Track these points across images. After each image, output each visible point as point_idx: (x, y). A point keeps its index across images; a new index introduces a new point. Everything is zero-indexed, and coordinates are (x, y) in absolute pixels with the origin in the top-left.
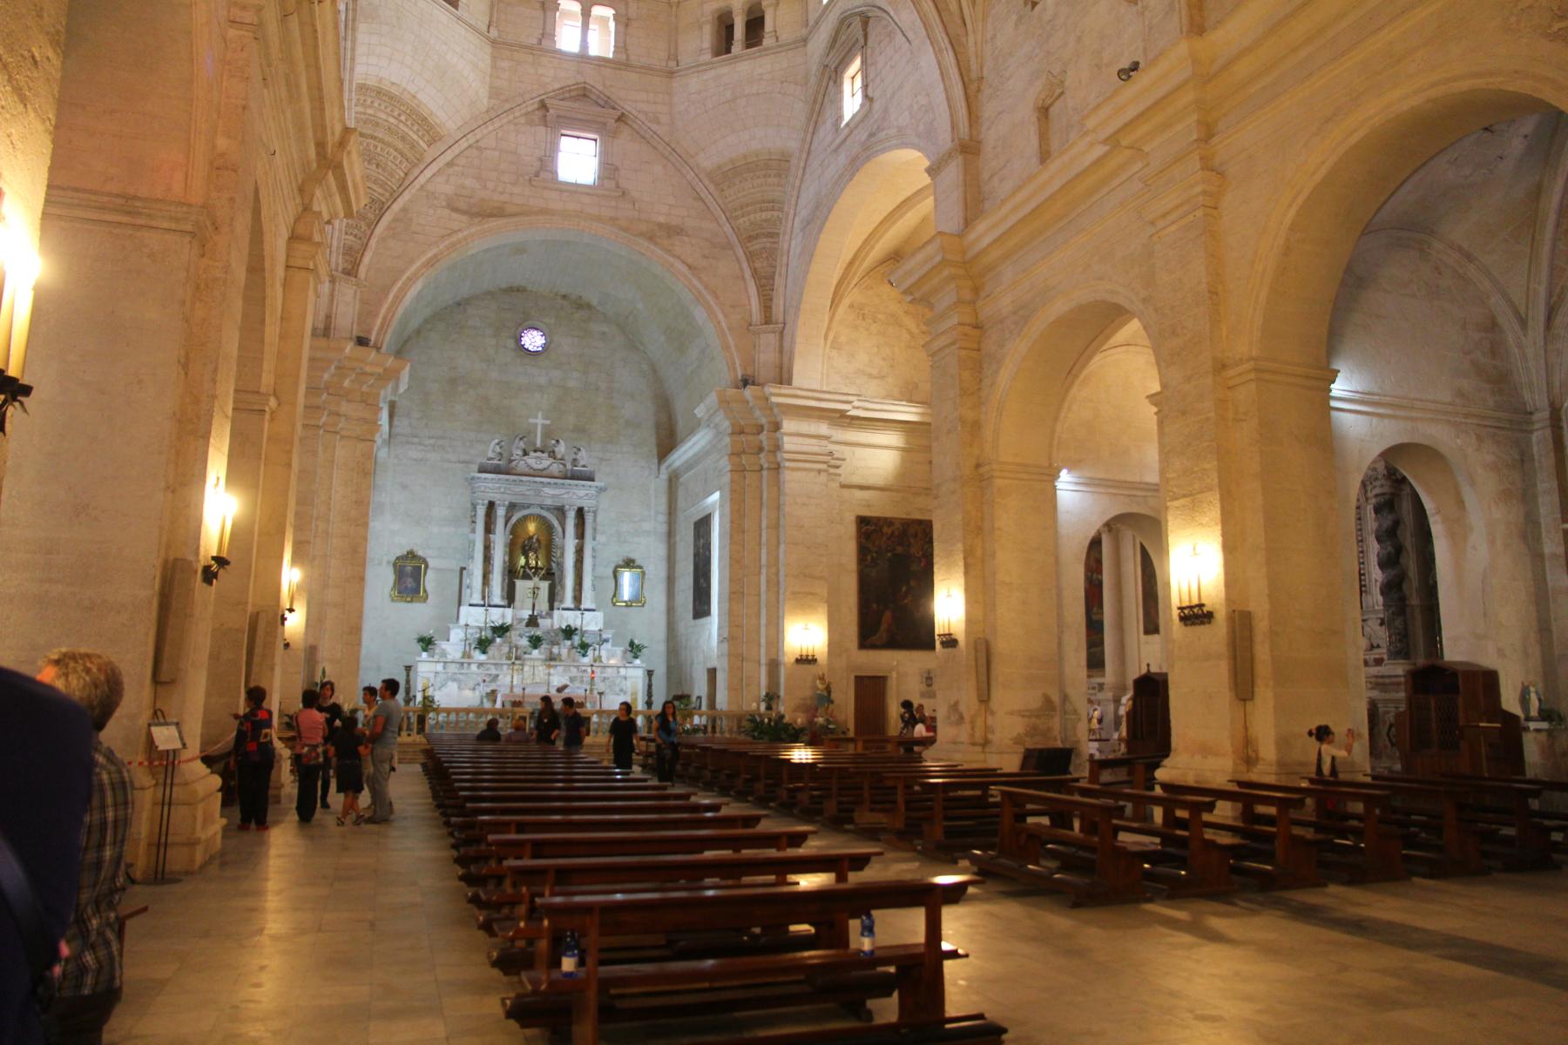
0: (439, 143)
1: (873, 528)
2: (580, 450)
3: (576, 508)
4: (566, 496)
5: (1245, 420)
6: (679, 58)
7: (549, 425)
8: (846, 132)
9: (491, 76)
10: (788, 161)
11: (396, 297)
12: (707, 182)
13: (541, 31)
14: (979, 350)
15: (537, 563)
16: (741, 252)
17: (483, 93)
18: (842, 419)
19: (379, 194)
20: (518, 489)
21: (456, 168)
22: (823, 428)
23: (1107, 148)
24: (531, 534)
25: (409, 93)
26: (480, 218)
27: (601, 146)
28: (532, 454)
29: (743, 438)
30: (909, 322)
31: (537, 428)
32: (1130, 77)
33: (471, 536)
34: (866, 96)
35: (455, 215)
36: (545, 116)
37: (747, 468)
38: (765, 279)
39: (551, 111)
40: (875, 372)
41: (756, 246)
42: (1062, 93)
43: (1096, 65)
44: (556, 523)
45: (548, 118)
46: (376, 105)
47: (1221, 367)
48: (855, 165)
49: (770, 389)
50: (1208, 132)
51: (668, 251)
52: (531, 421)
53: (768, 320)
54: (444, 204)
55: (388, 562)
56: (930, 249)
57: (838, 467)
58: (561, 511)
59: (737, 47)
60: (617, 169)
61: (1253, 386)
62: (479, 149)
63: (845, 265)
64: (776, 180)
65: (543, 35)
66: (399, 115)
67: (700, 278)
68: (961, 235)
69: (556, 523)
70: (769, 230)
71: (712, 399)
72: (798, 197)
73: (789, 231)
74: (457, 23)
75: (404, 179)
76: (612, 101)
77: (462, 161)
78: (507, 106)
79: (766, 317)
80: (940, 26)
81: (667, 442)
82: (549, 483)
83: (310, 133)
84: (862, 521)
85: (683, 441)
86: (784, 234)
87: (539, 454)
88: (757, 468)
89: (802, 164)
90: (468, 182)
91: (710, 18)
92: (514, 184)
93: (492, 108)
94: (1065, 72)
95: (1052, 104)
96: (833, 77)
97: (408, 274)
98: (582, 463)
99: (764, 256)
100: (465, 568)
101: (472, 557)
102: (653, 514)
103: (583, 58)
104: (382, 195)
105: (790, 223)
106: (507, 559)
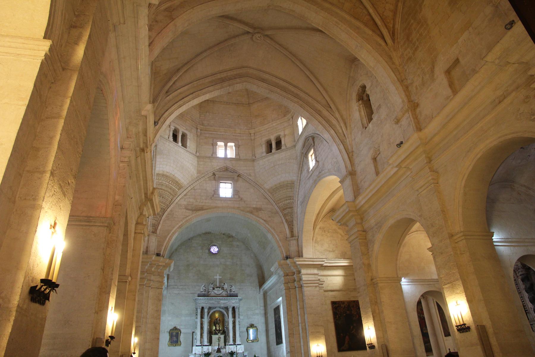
0: (182, 189)
1: (337, 305)
2: (232, 286)
3: (232, 307)
4: (228, 303)
5: (464, 253)
6: (256, 155)
7: (221, 278)
8: (311, 172)
9: (197, 167)
10: (294, 183)
11: (169, 239)
12: (268, 193)
13: (212, 152)
14: (366, 239)
15: (219, 328)
16: (281, 214)
17: (195, 172)
18: (322, 267)
19: (163, 206)
20: (211, 302)
21: (187, 196)
22: (315, 271)
23: (398, 169)
24: (217, 318)
25: (172, 174)
26: (195, 211)
27: (233, 185)
28: (216, 289)
29: (288, 277)
30: (340, 231)
31: (217, 279)
32: (401, 146)
33: (196, 320)
34: (316, 161)
35: (187, 211)
36: (215, 177)
37: (291, 288)
38: (290, 222)
39: (216, 176)
40: (331, 250)
41: (286, 212)
42: (380, 153)
43: (389, 143)
44: (225, 313)
45: (216, 178)
46: (162, 179)
47: (451, 236)
48: (316, 182)
49: (296, 259)
50: (430, 160)
51: (258, 216)
52: (215, 277)
53: (292, 236)
54: (184, 208)
55: (167, 332)
56: (345, 207)
57: (322, 284)
58: (227, 309)
59: (274, 150)
60: (239, 191)
61: (464, 241)
62: (194, 189)
63: (316, 215)
64: (290, 190)
65: (213, 153)
66: (169, 182)
67: (268, 224)
68: (354, 201)
69: (225, 313)
70: (290, 206)
71: (276, 264)
72: (298, 195)
73: (296, 205)
74: (187, 152)
75: (171, 201)
76: (236, 171)
77: (189, 194)
78: (203, 175)
79: (292, 235)
80: (337, 138)
81: (262, 281)
82: (222, 299)
83: (143, 191)
84: (333, 303)
85: (267, 280)
86: (295, 207)
87: (218, 289)
88: (294, 287)
89: (298, 184)
90: (191, 200)
91: (264, 143)
92: (206, 199)
93: (198, 177)
94: (379, 146)
95: (377, 157)
96: (305, 156)
97: (173, 231)
98: (233, 291)
99: (289, 215)
100: (194, 332)
101: (197, 328)
102: (259, 307)
103: (226, 159)
104: (164, 207)
105: (296, 203)
106: (209, 327)
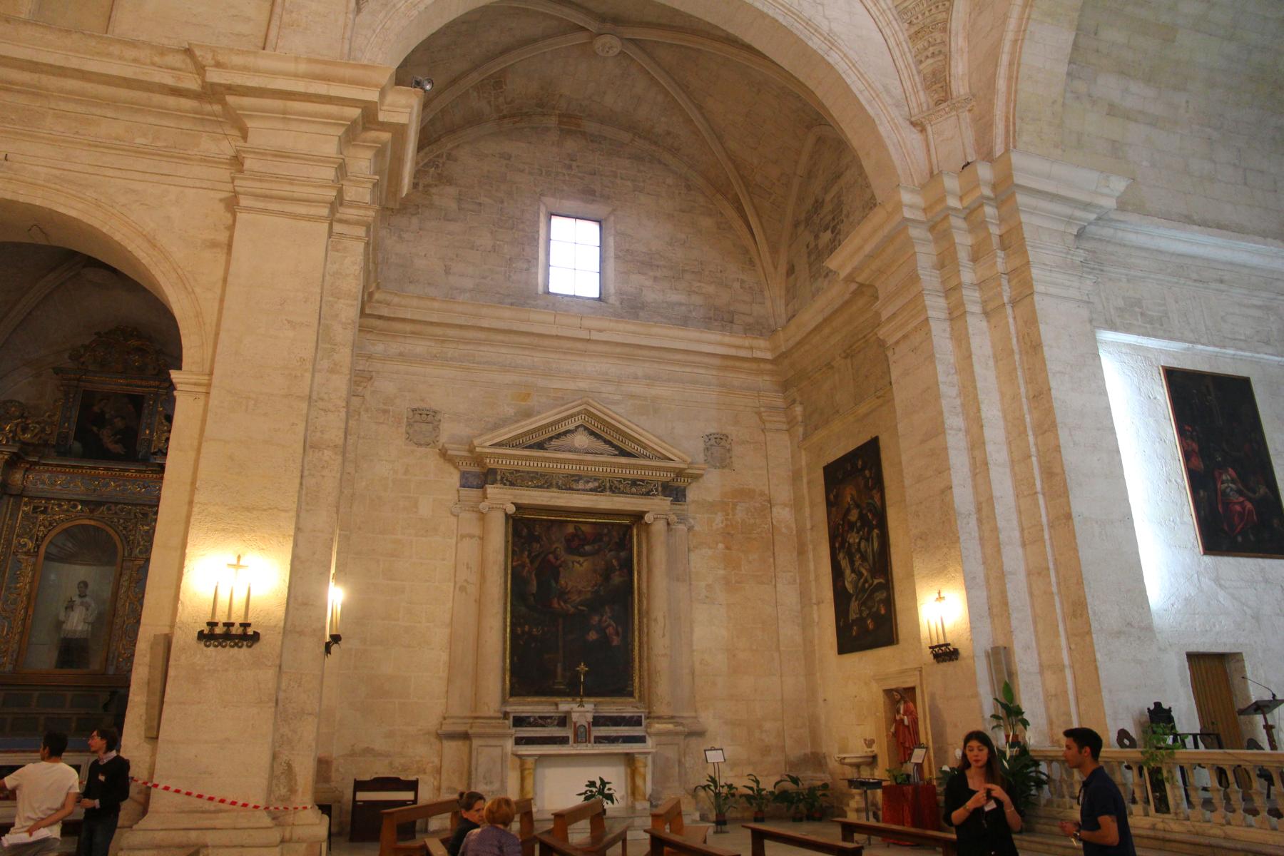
97: (1010, 36)
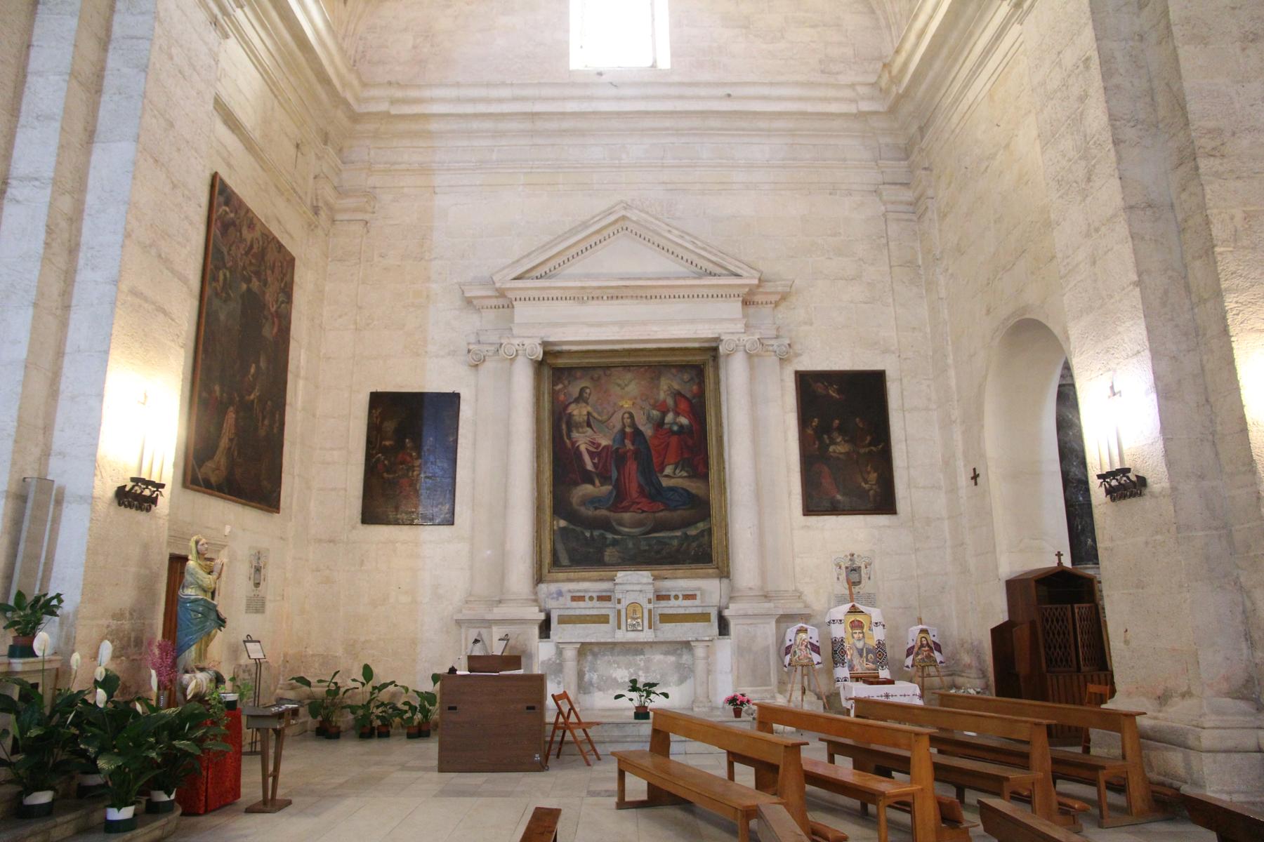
1: (232, 215)
